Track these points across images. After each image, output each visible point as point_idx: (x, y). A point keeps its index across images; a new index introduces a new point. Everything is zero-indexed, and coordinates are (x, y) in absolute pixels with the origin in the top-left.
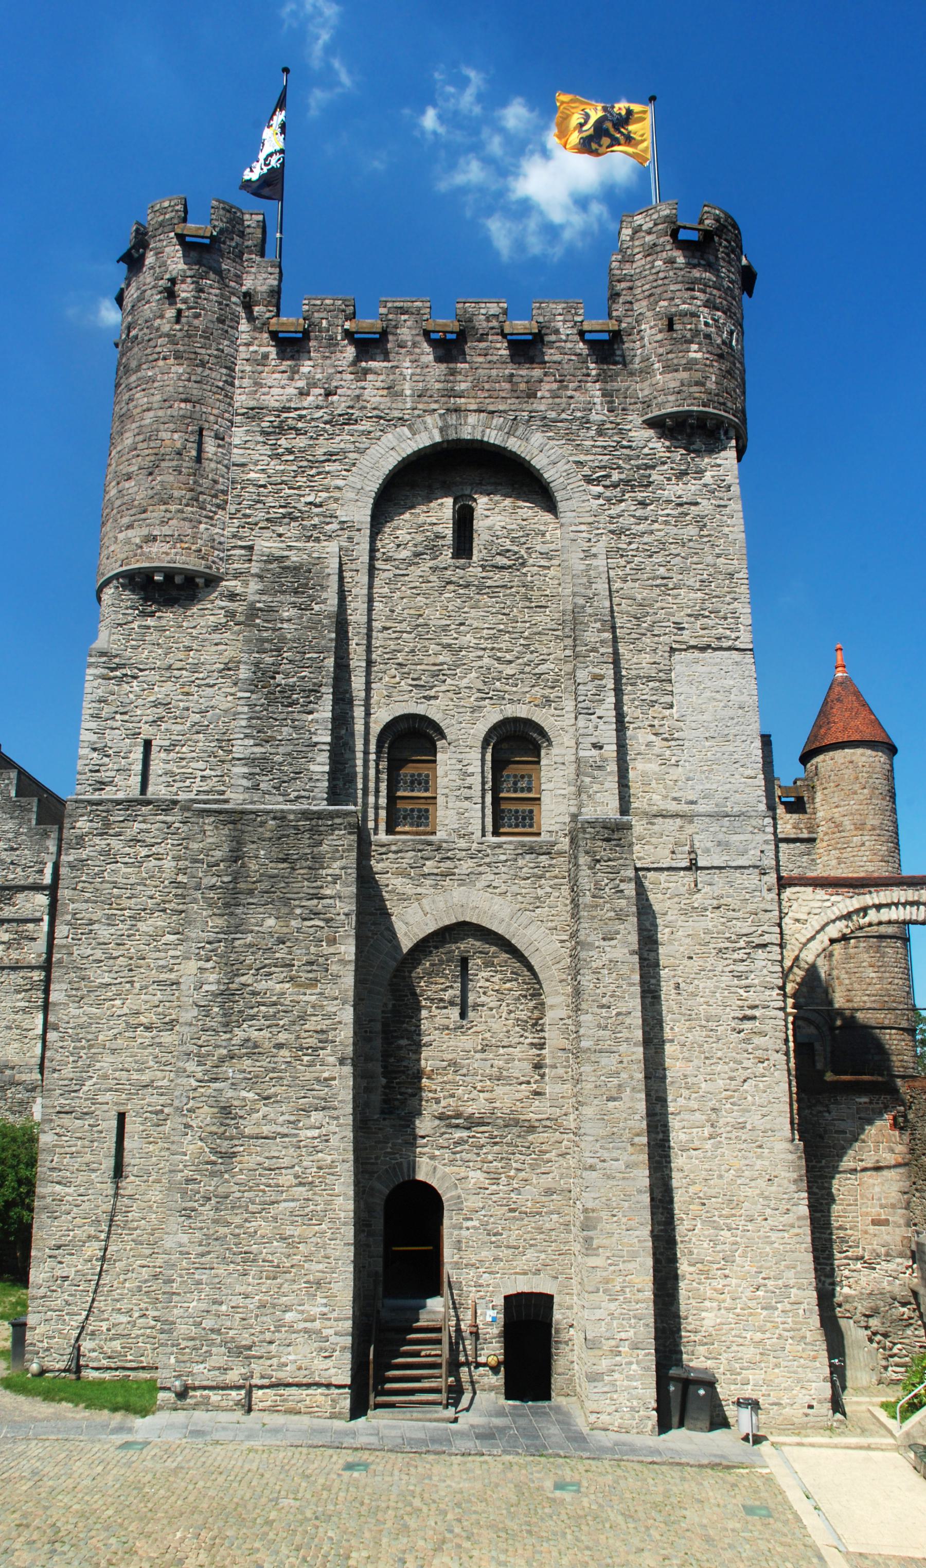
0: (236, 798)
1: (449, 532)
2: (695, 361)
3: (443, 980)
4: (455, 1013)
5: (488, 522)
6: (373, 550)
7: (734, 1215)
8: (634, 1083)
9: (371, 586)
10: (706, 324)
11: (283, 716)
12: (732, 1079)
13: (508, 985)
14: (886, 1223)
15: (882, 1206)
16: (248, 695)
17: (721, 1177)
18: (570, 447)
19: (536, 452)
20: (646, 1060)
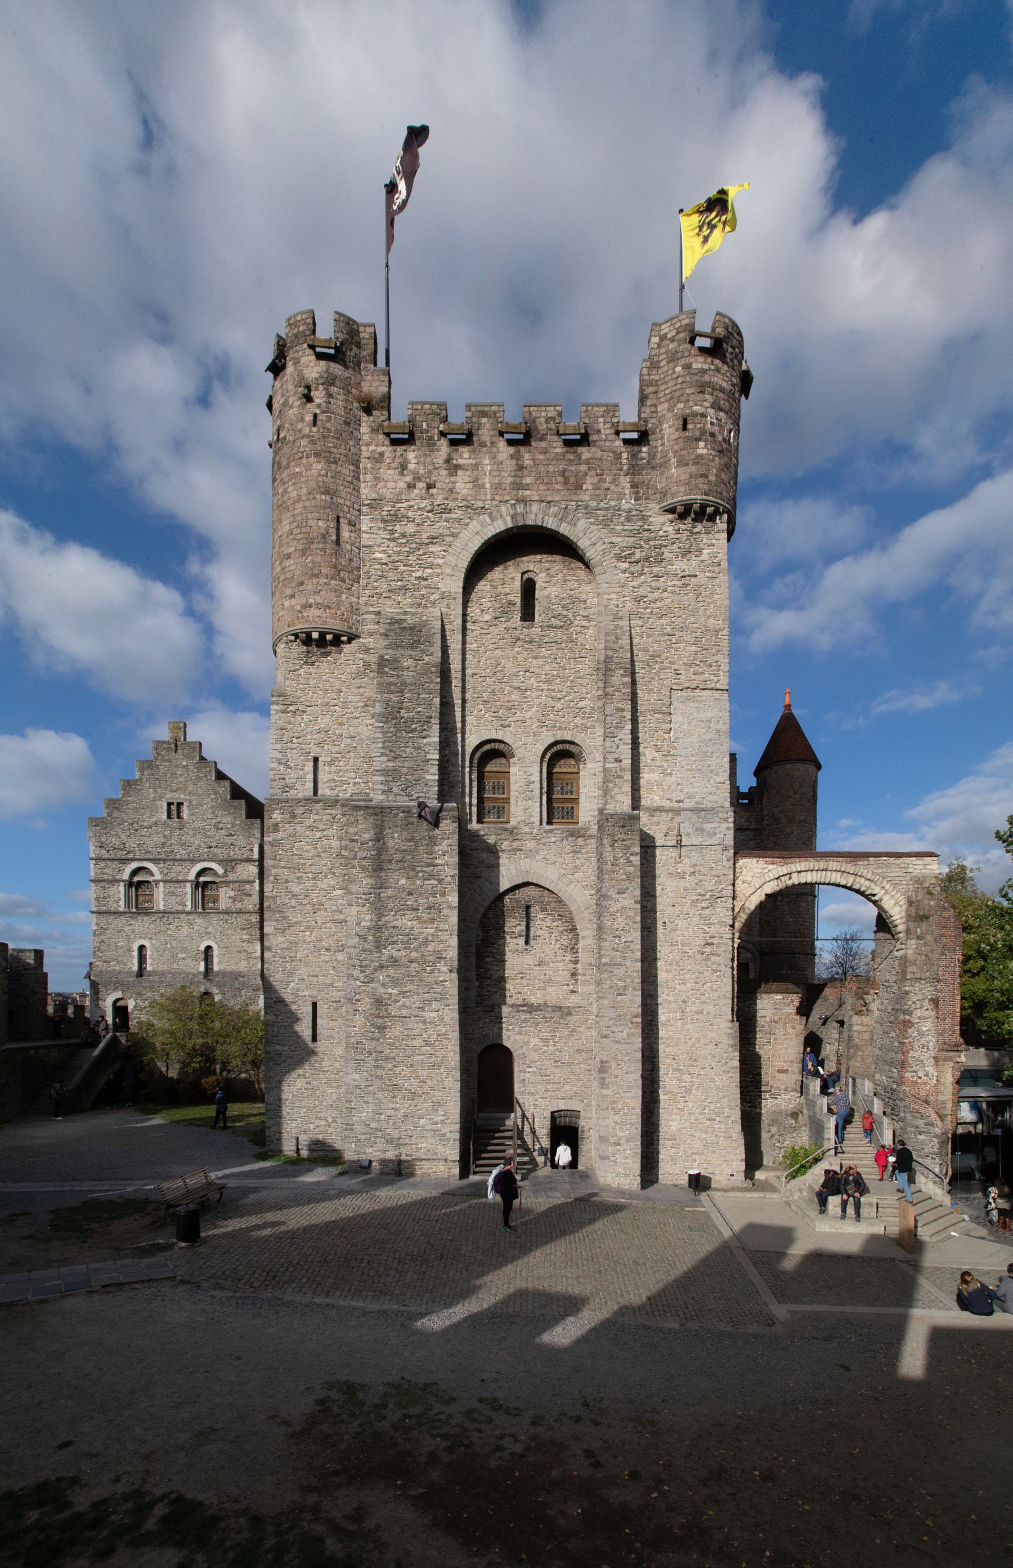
0: (378, 798)
1: (518, 600)
2: (701, 456)
3: (514, 920)
4: (522, 941)
5: (545, 593)
6: (465, 615)
7: (693, 1066)
8: (635, 985)
9: (464, 643)
10: (712, 424)
11: (406, 740)
12: (696, 983)
13: (556, 924)
14: (786, 1071)
15: (785, 1062)
16: (382, 725)
17: (686, 1043)
18: (606, 531)
19: (581, 535)
20: (643, 971)
